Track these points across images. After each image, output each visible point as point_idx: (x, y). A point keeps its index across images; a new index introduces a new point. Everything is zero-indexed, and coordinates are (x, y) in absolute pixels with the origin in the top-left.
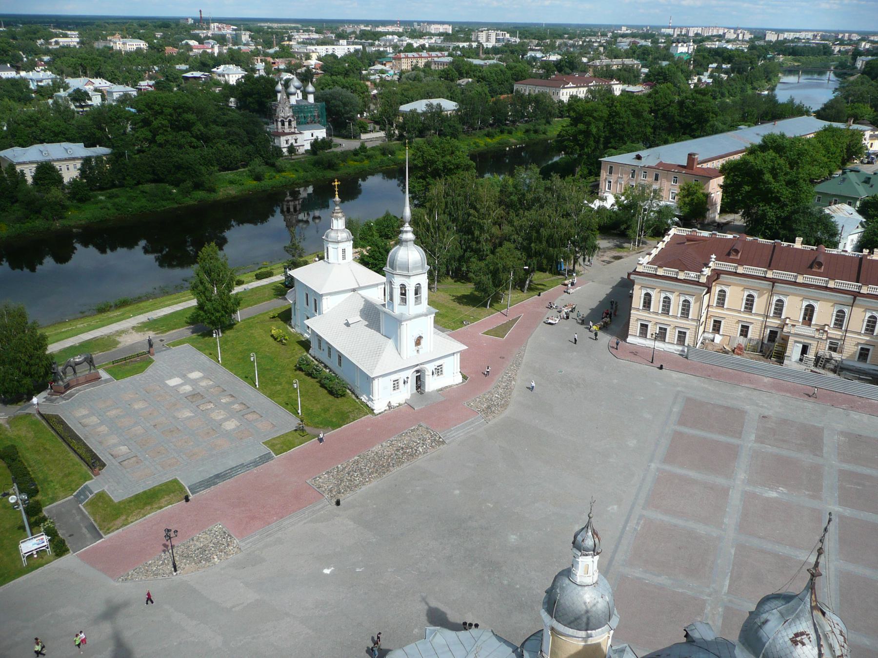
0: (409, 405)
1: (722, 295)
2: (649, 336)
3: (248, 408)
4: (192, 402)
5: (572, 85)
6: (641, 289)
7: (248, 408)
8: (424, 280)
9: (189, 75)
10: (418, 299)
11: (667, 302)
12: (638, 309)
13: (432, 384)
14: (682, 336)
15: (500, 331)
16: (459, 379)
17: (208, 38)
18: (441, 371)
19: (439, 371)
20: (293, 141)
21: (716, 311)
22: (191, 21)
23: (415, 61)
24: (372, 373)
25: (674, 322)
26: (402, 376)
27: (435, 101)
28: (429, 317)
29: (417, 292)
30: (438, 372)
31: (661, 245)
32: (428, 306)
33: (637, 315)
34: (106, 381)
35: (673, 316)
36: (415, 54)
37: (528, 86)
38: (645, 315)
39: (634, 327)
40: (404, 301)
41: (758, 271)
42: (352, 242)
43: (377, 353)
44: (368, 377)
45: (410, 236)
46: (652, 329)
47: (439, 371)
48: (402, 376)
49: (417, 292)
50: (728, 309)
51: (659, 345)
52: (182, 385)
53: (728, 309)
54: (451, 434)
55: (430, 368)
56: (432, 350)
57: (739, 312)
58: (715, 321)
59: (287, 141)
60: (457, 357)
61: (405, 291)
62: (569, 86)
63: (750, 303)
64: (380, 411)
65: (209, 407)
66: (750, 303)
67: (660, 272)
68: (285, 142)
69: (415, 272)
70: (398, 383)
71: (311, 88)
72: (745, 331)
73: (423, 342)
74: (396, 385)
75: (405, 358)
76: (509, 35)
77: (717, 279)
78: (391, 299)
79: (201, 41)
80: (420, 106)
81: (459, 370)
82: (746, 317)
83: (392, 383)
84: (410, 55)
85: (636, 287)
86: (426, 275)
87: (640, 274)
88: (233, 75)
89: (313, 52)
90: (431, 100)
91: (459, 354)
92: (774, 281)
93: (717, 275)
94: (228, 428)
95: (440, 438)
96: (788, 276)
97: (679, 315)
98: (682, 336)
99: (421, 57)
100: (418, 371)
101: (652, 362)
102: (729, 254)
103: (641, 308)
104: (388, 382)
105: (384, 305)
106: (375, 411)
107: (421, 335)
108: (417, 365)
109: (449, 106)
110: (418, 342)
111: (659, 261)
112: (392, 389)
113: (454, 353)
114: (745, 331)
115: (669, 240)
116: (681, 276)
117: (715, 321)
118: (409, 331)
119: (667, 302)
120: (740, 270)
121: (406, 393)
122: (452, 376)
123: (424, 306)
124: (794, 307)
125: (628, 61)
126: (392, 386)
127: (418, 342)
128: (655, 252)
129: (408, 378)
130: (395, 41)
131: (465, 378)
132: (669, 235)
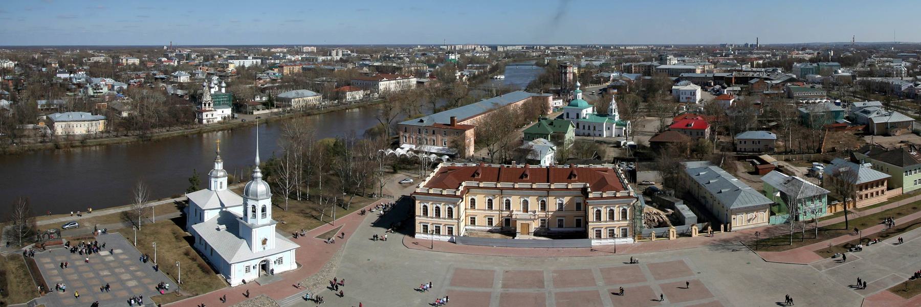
0: (256, 282)
1: (473, 202)
6: (420, 203)
8: (268, 203)
11: (438, 210)
12: (420, 216)
14: (450, 231)
15: (326, 237)
16: (295, 267)
18: (282, 261)
19: (280, 261)
21: (471, 212)
24: (230, 260)
25: (444, 221)
26: (253, 263)
28: (272, 226)
29: (264, 210)
30: (279, 262)
31: (432, 175)
33: (419, 220)
35: (443, 218)
38: (424, 219)
39: (419, 228)
40: (254, 216)
41: (491, 184)
43: (235, 249)
44: (228, 264)
47: (280, 261)
48: (253, 263)
49: (264, 210)
50: (478, 209)
51: (436, 237)
52: (115, 268)
53: (478, 209)
55: (272, 259)
56: (274, 247)
57: (485, 210)
58: (471, 218)
63: (490, 203)
66: (490, 203)
67: (431, 191)
70: (249, 268)
72: (490, 222)
73: (267, 242)
74: (248, 269)
75: (255, 252)
77: (468, 192)
81: (295, 261)
82: (489, 213)
83: (245, 268)
85: (417, 202)
87: (418, 194)
92: (501, 189)
93: (468, 189)
94: (130, 285)
95: (276, 303)
96: (509, 185)
97: (447, 217)
98: (450, 231)
100: (265, 261)
102: (473, 176)
103: (422, 215)
104: (241, 266)
105: (241, 218)
107: (266, 238)
110: (264, 242)
111: (431, 185)
112: (245, 271)
113: (290, 250)
114: (490, 222)
116: (445, 192)
117: (471, 218)
118: (257, 235)
119: (438, 210)
120: (481, 185)
121: (254, 275)
122: (289, 264)
123: (269, 217)
124: (516, 203)
126: (245, 270)
127: (264, 242)
128: (428, 179)
129: (256, 265)
132: (437, 168)
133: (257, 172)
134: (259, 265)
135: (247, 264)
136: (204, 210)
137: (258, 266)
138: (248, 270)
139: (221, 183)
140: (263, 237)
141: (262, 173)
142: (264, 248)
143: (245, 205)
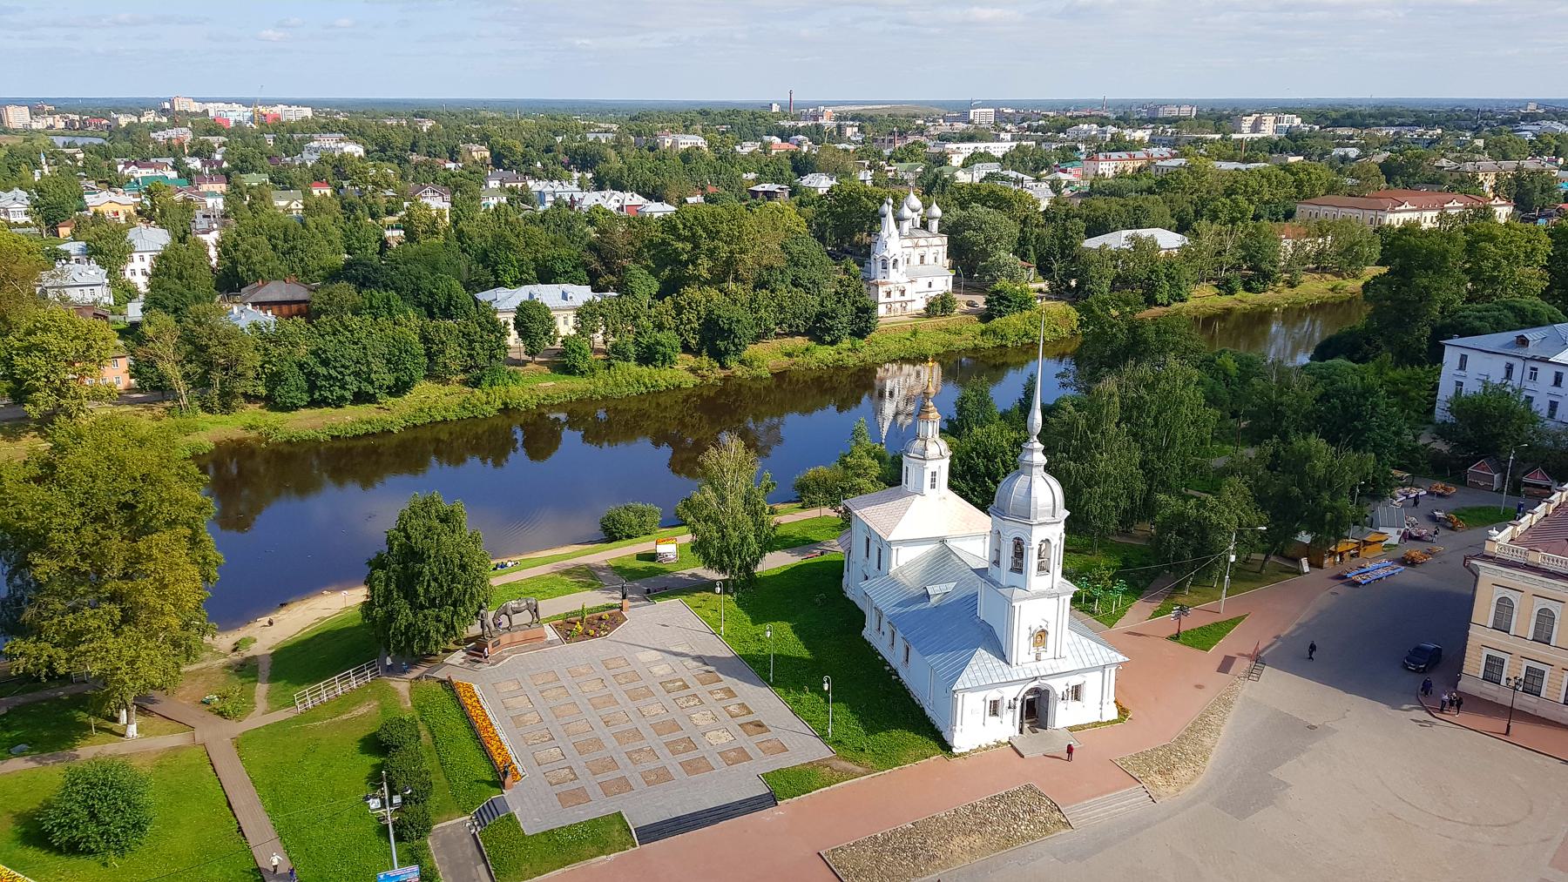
2: (1503, 682)
3: (750, 712)
4: (668, 692)
5: (1409, 207)
7: (750, 712)
9: (758, 188)
10: (1043, 568)
13: (1064, 715)
16: (1111, 713)
17: (798, 131)
20: (898, 293)
22: (775, 108)
23: (1121, 166)
27: (1144, 233)
32: (1063, 580)
34: (551, 643)
36: (1124, 155)
37: (1323, 208)
38: (1498, 638)
40: (1018, 568)
42: (947, 461)
45: (1039, 458)
46: (1513, 669)
47: (1076, 693)
54: (1083, 812)
55: (1059, 686)
59: (889, 295)
60: (1111, 674)
61: (1022, 550)
62: (1403, 207)
64: (963, 751)
65: (692, 703)
67: (1537, 558)
68: (885, 294)
69: (1041, 519)
71: (936, 211)
73: (1050, 638)
76: (1300, 119)
78: (997, 563)
79: (785, 135)
80: (1118, 240)
84: (1115, 155)
86: (1062, 526)
88: (821, 183)
89: (954, 152)
90: (1138, 231)
91: (1113, 669)
99: (1132, 158)
100: (1036, 691)
101: (1507, 733)
106: (954, 750)
108: (1036, 679)
109: (1168, 240)
111: (1535, 537)
115: (1564, 499)
121: (1007, 727)
125: (1530, 164)
130: (1093, 133)
131: (1123, 711)
133: (1032, 450)
134: (1023, 700)
135: (993, 695)
136: (889, 544)
137: (1019, 704)
138: (994, 708)
139: (934, 474)
140: (1036, 627)
141: (1045, 452)
142: (1038, 659)
143: (997, 534)
